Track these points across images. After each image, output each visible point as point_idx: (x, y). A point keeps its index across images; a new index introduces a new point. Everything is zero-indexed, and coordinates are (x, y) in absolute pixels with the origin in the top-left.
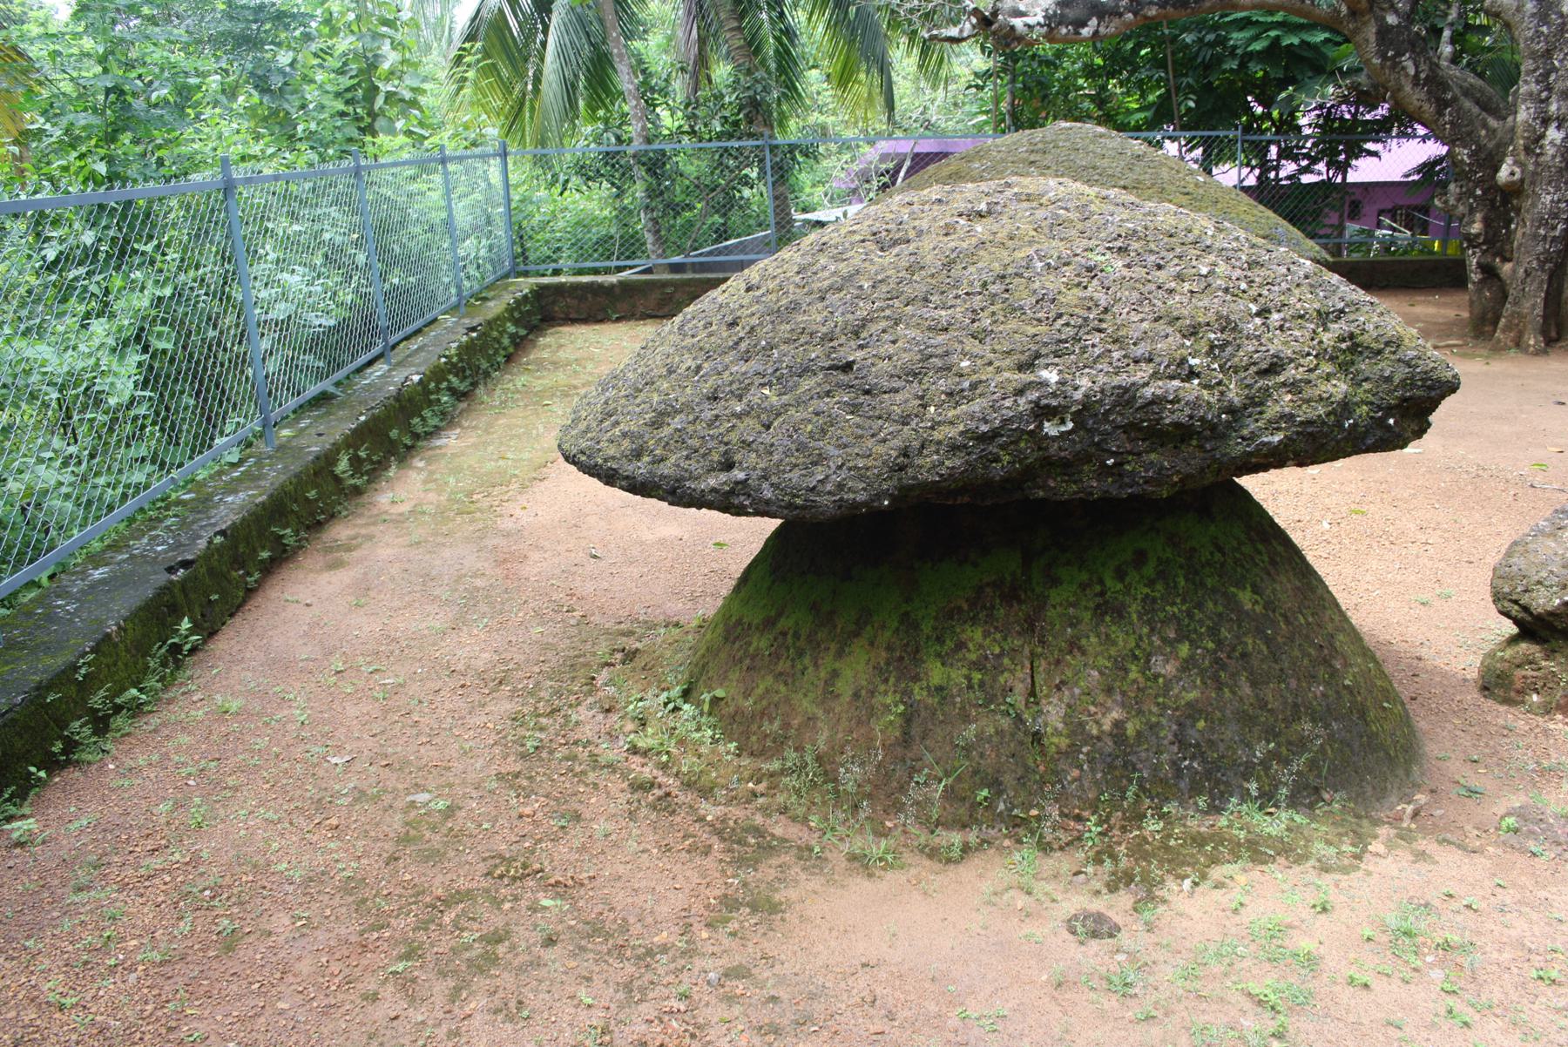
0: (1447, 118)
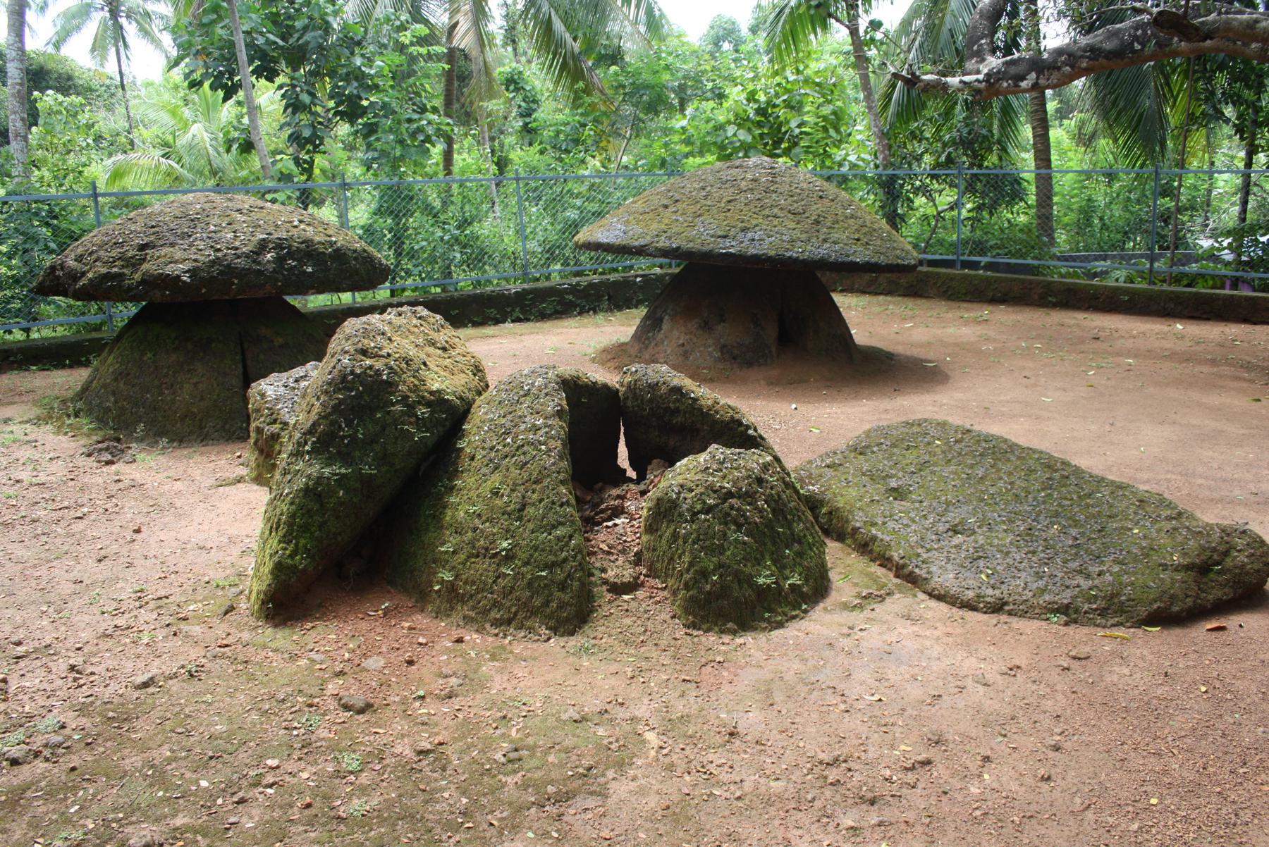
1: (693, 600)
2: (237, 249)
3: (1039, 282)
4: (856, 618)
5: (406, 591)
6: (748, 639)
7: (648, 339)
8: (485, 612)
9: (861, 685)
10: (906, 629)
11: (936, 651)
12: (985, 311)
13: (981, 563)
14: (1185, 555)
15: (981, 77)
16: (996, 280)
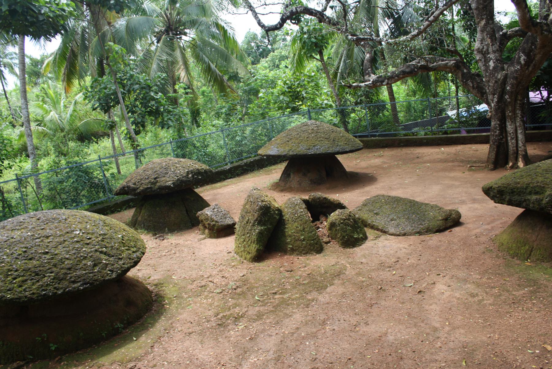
0: (485, 98)
1: (343, 242)
2: (182, 175)
3: (397, 139)
4: (375, 241)
5: (280, 252)
6: (355, 249)
7: (287, 180)
8: (301, 252)
9: (381, 251)
10: (387, 242)
11: (394, 244)
12: (381, 152)
13: (399, 226)
14: (442, 217)
15: (371, 82)
16: (383, 140)
